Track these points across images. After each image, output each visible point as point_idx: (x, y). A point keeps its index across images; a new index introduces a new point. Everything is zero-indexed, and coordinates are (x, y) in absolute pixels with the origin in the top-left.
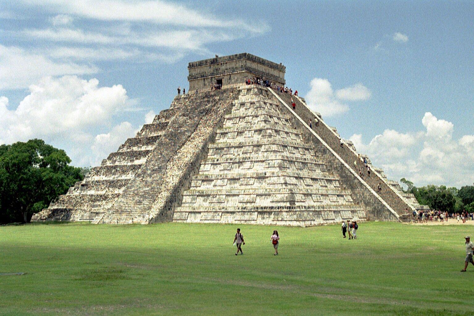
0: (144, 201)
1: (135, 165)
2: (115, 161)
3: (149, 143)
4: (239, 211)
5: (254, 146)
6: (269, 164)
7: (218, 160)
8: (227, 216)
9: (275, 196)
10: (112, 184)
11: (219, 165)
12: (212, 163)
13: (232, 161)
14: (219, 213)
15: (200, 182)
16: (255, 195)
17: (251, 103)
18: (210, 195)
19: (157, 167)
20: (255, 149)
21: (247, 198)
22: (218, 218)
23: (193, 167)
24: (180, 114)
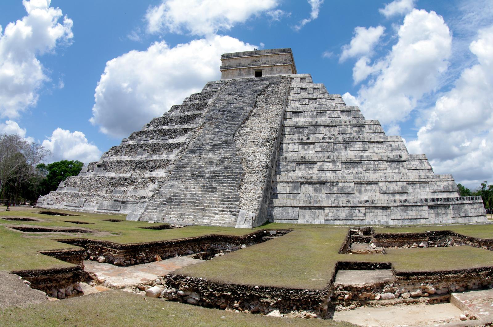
0: (219, 186)
1: (171, 144)
2: (140, 140)
3: (184, 122)
4: (396, 205)
5: (354, 126)
6: (391, 145)
7: (308, 139)
8: (375, 214)
9: (435, 184)
10: (141, 165)
11: (312, 145)
12: (300, 141)
13: (332, 141)
14: (360, 208)
15: (295, 165)
16: (405, 183)
17: (315, 88)
18: (326, 182)
19: (218, 142)
20: (355, 129)
21: (393, 187)
22: (361, 216)
23: (277, 144)
24: (224, 93)
